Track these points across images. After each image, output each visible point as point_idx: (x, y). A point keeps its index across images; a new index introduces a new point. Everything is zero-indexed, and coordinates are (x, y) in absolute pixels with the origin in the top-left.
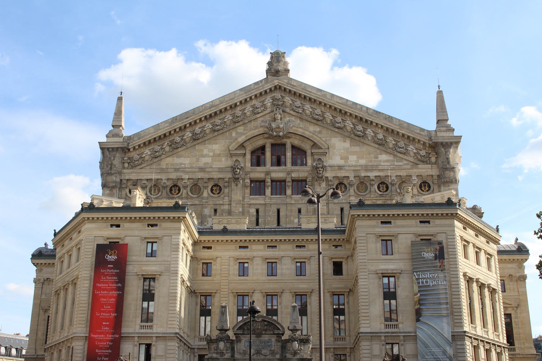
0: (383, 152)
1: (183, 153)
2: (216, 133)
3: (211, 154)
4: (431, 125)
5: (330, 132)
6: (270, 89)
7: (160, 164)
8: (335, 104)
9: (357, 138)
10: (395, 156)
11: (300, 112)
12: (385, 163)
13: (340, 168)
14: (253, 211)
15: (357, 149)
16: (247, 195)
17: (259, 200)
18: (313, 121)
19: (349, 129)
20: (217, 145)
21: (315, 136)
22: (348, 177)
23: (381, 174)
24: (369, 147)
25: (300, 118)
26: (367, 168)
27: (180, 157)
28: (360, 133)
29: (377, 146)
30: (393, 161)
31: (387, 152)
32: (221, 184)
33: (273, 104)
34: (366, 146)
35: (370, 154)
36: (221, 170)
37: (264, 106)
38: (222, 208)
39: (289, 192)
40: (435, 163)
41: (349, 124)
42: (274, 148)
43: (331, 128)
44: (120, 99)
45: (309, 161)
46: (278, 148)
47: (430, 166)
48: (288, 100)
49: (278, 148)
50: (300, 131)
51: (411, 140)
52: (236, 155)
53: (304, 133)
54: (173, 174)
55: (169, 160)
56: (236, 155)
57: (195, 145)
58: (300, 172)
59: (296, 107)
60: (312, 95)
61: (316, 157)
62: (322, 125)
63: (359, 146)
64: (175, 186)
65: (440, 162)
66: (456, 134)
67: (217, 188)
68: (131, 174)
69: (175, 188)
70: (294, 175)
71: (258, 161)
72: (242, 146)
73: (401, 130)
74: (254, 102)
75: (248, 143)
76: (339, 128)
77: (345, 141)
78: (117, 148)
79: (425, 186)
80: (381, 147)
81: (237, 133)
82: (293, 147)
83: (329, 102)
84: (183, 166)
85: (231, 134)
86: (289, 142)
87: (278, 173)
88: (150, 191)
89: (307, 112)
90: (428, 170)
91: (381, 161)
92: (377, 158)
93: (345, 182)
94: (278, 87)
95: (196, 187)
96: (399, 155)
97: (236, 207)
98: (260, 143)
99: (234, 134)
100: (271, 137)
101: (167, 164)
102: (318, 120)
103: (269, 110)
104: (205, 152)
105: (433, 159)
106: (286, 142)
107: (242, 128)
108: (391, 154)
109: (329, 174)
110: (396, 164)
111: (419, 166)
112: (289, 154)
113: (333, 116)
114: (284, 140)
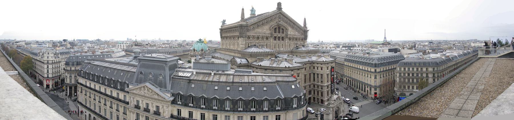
4: (303, 26)
12: (297, 34)
17: (275, 42)
26: (294, 35)
36: (268, 34)
44: (243, 9)
46: (279, 28)
49: (279, 28)
58: (283, 35)
67: (267, 38)
68: (248, 34)
71: (275, 32)
87: (279, 35)
90: (303, 36)
95: (263, 38)
102: (286, 23)
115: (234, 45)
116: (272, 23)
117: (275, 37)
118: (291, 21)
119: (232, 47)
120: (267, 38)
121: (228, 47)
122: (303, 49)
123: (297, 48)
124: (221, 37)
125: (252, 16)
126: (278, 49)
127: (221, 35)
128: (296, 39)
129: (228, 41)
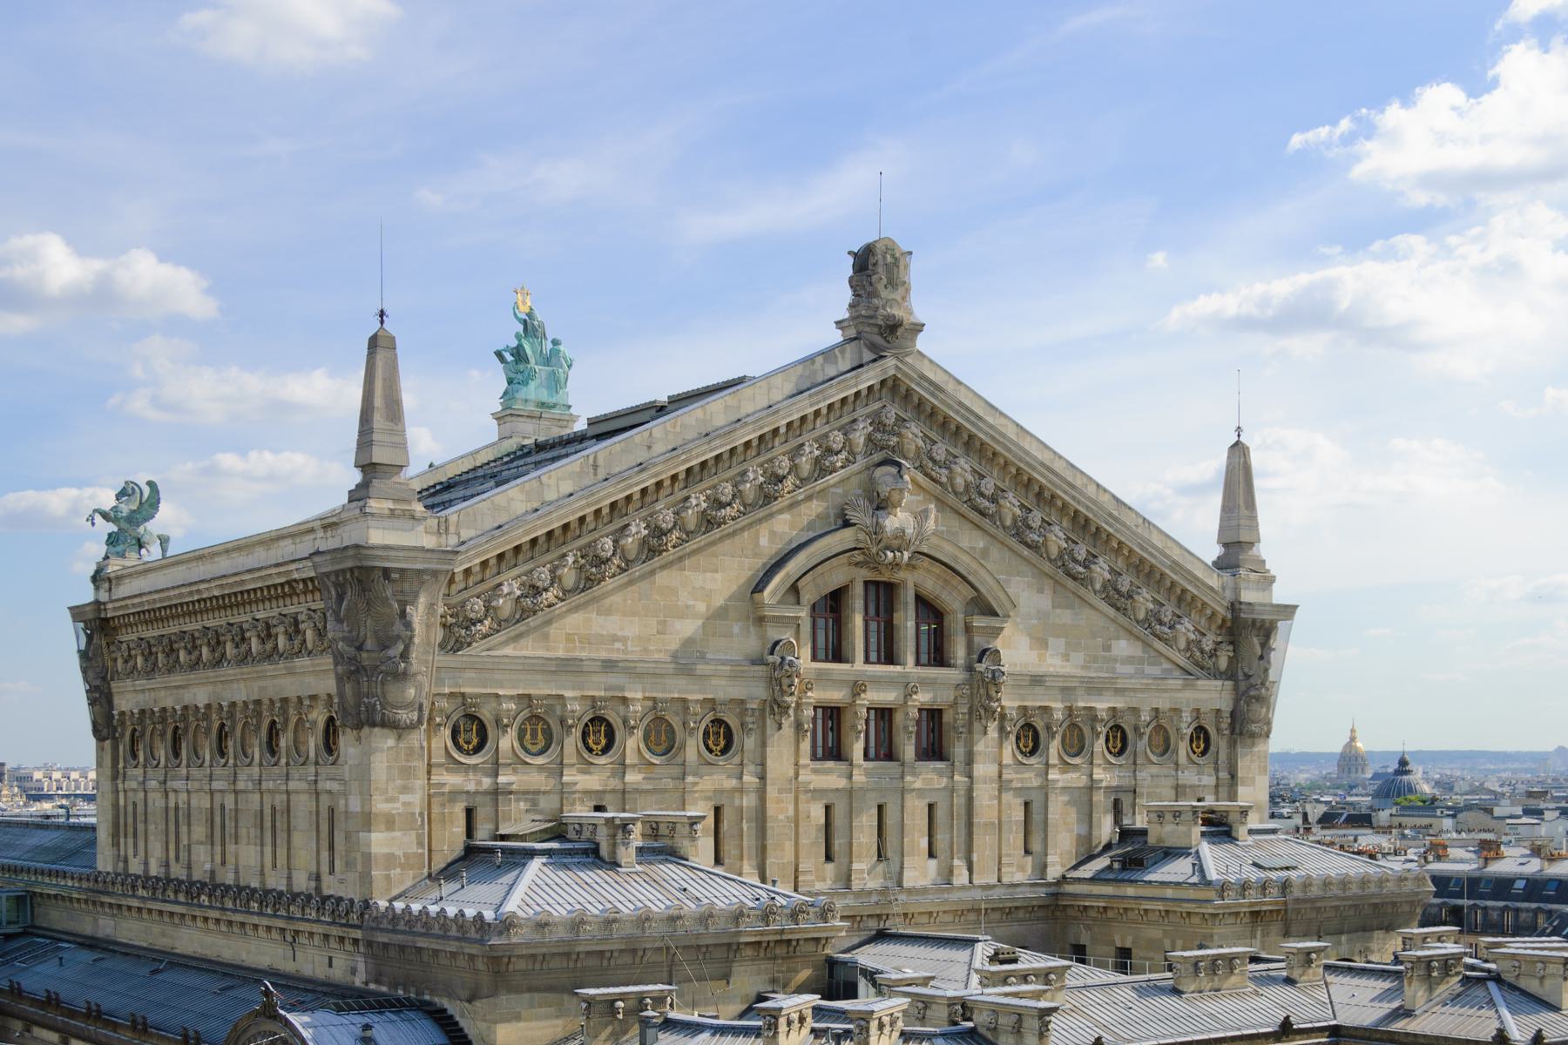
0: (1122, 632)
1: (617, 598)
2: (716, 533)
3: (701, 607)
4: (1210, 551)
5: (1008, 554)
6: (870, 388)
7: (546, 637)
8: (1034, 469)
9: (1070, 583)
10: (1147, 645)
11: (944, 479)
13: (1037, 680)
14: (818, 813)
15: (1065, 617)
16: (805, 760)
17: (830, 777)
18: (974, 515)
19: (1054, 551)
20: (718, 576)
21: (982, 572)
22: (1046, 710)
23: (1119, 704)
24: (1092, 612)
25: (938, 500)
27: (608, 612)
28: (1081, 569)
29: (1111, 612)
30: (1141, 661)
31: (1131, 633)
32: (733, 723)
33: (869, 438)
34: (1088, 611)
35: (1094, 636)
37: (848, 444)
38: (737, 803)
39: (909, 750)
40: (1230, 674)
41: (1057, 539)
42: (874, 604)
43: (1013, 542)
45: (959, 652)
46: (883, 595)
47: (1219, 683)
48: (914, 434)
50: (946, 552)
51: (1184, 600)
52: (780, 621)
53: (955, 558)
54: (595, 678)
55: (574, 622)
56: (780, 621)
57: (652, 572)
59: (931, 459)
60: (980, 429)
61: (980, 641)
62: (993, 530)
63: (1070, 607)
64: (597, 720)
65: (1241, 677)
66: (1279, 595)
69: (600, 732)
70: (923, 698)
72: (794, 589)
73: (1173, 571)
74: (821, 428)
75: (809, 577)
76: (1029, 546)
77: (1041, 591)
78: (419, 572)
79: (1198, 738)
80: (1121, 618)
81: (773, 534)
82: (921, 600)
83: (1021, 460)
84: (618, 645)
85: (757, 538)
86: (911, 581)
88: (521, 738)
89: (959, 481)
90: (1213, 695)
91: (1115, 660)
92: (1108, 648)
93: (1039, 724)
94: (890, 383)
96: (1158, 645)
97: (779, 801)
98: (835, 577)
99: (764, 541)
100: (871, 562)
101: (569, 638)
103: (861, 462)
104: (684, 598)
105: (1223, 663)
106: (904, 581)
107: (786, 516)
108: (1138, 638)
109: (1009, 701)
110: (1149, 670)
111: (1200, 682)
112: (907, 622)
113: (1022, 506)
114: (901, 575)
115: (275, 825)
116: (782, 527)
117: (833, 715)
118: (1043, 497)
119: (247, 861)
120: (721, 737)
121: (203, 862)
122: (1216, 860)
123: (1135, 853)
124: (105, 726)
125: (530, 433)
126: (867, 875)
127: (100, 697)
128: (1120, 740)
129: (196, 787)
